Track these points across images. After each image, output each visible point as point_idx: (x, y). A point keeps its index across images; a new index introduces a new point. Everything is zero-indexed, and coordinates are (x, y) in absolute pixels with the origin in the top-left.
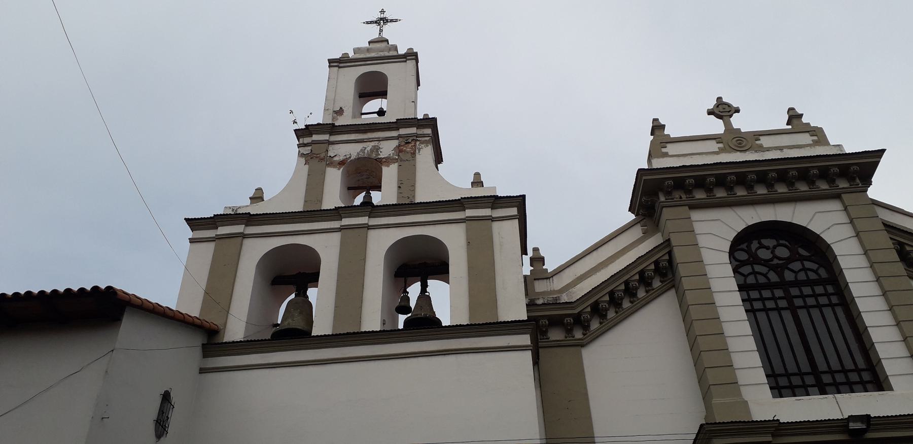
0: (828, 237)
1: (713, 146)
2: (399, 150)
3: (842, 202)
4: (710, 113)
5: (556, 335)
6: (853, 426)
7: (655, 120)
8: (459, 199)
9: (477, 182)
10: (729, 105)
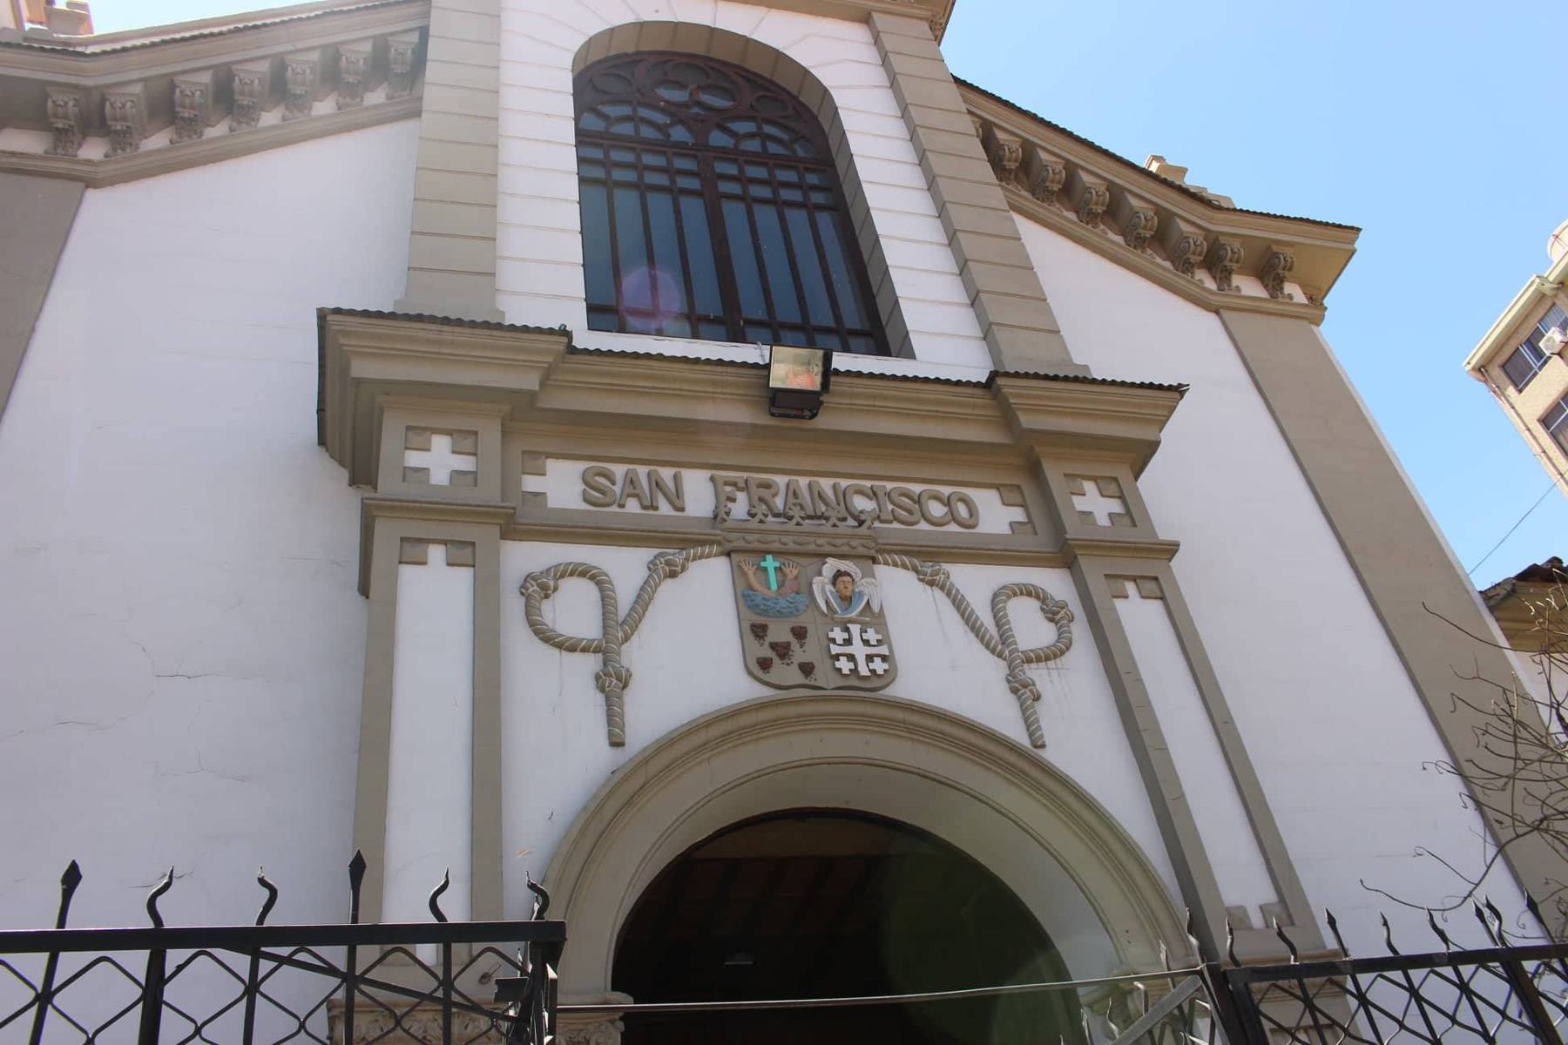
3: (869, 27)
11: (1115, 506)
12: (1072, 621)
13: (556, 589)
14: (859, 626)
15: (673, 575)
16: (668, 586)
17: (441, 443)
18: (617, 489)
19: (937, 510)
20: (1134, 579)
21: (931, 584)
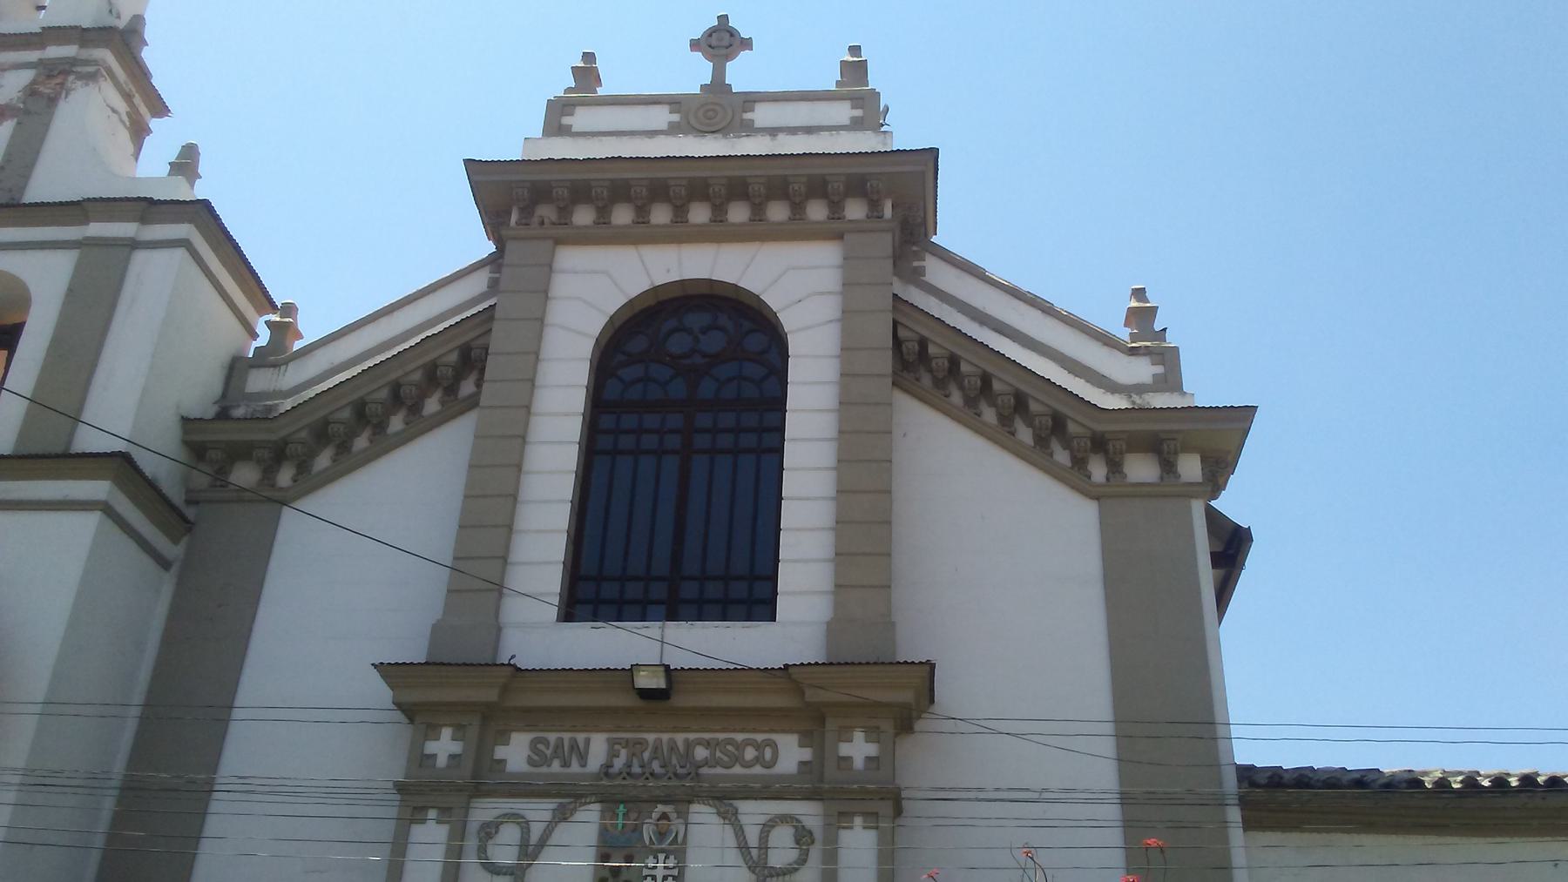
0: (788, 321)
1: (661, 117)
2: (31, 92)
4: (695, 45)
5: (245, 475)
6: (645, 680)
7: (589, 57)
8: (79, 201)
9: (187, 163)
10: (732, 33)
11: (872, 749)
12: (813, 842)
13: (496, 832)
14: (665, 855)
15: (565, 819)
16: (562, 826)
17: (446, 733)
18: (548, 752)
19: (750, 754)
20: (865, 814)
21: (724, 818)
